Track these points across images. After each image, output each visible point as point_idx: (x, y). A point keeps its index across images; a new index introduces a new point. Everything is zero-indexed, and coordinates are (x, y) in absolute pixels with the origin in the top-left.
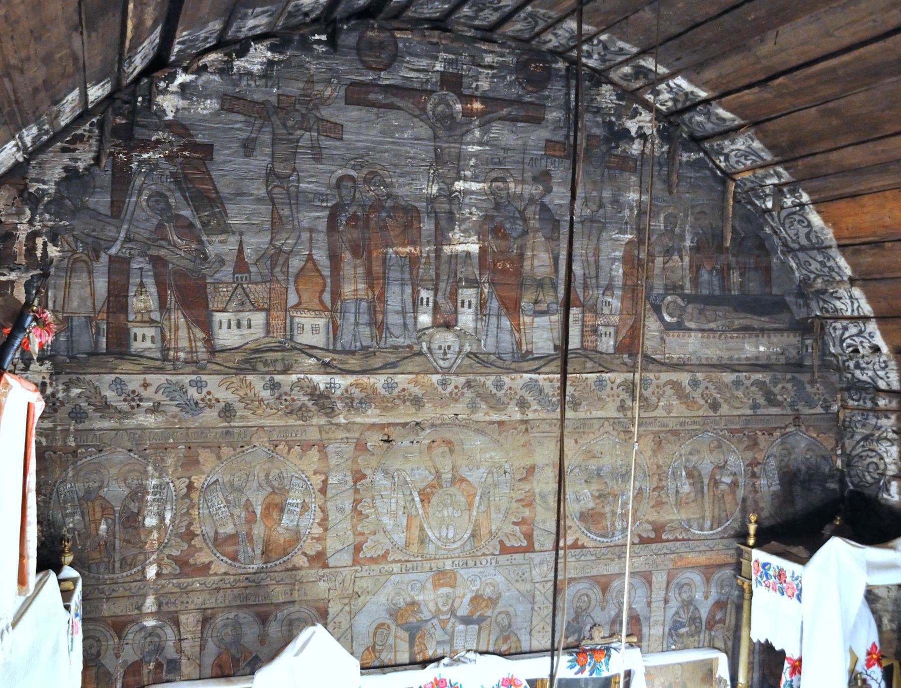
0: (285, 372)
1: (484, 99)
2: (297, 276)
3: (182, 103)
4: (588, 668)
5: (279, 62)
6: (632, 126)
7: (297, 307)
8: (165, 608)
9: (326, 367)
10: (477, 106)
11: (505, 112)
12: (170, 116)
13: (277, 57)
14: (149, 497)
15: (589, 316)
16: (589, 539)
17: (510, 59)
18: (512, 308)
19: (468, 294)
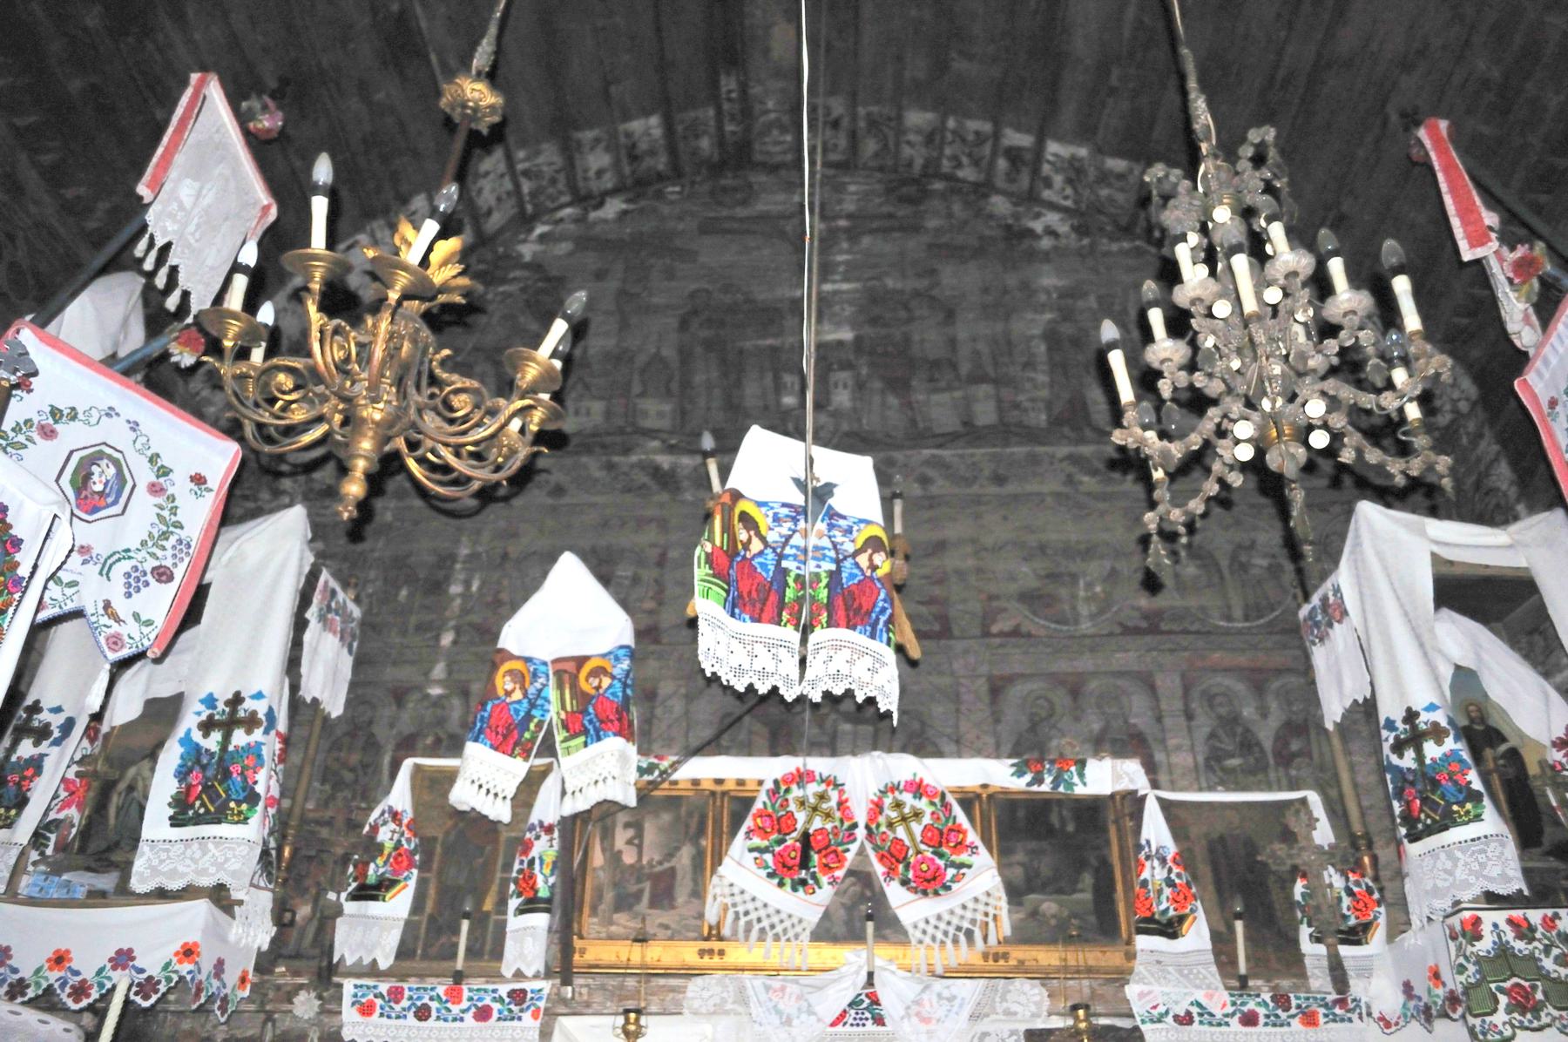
0: (627, 451)
1: (849, 216)
2: (643, 371)
3: (538, 248)
4: (1048, 779)
5: (632, 211)
6: (1038, 226)
7: (643, 395)
8: (456, 676)
9: (671, 449)
10: (842, 223)
11: (875, 225)
12: (528, 258)
13: (631, 207)
14: (458, 566)
15: (1006, 393)
16: (1036, 625)
17: (877, 186)
18: (898, 385)
19: (844, 376)
